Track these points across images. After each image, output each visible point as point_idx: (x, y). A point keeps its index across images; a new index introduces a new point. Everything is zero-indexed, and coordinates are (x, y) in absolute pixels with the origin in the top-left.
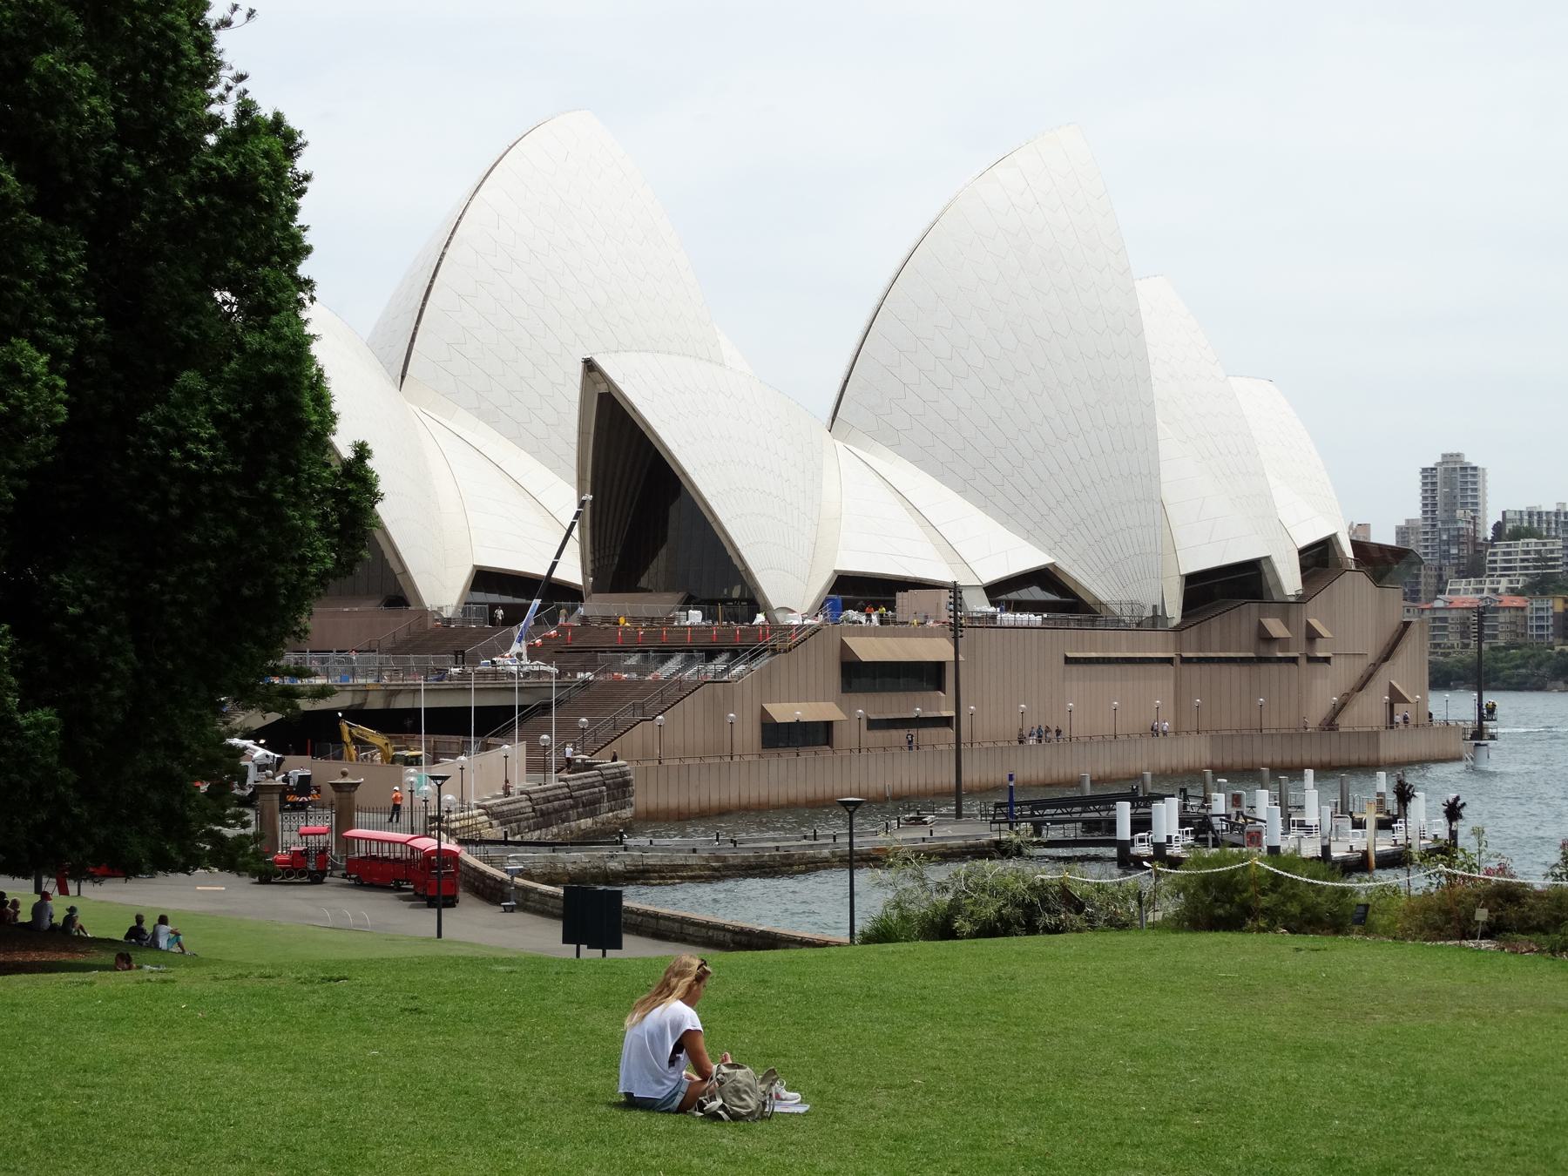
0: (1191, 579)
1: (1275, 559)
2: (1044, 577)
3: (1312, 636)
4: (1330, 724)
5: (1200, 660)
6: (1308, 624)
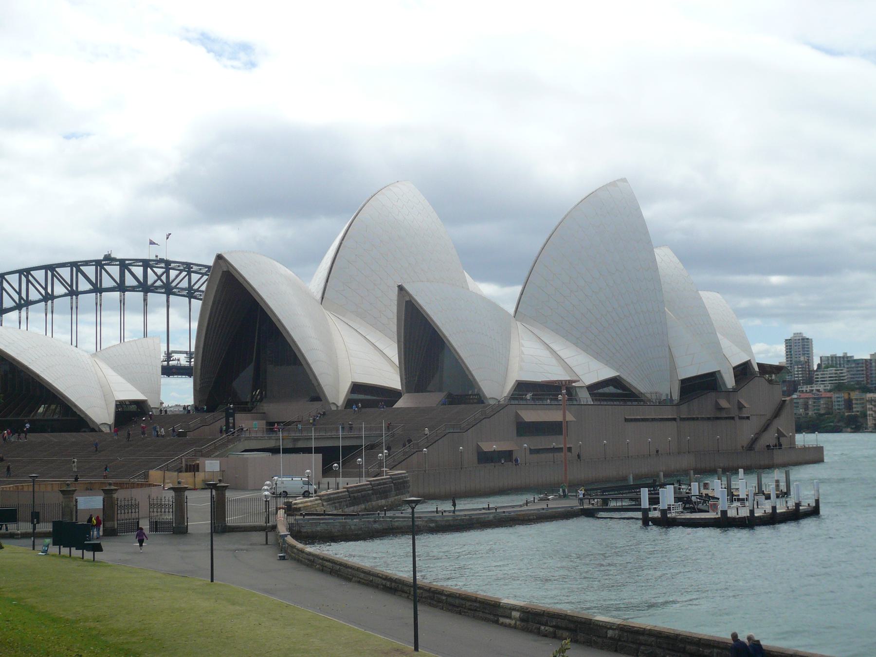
0: (683, 382)
1: (722, 372)
2: (615, 382)
3: (741, 407)
4: (751, 447)
5: (688, 419)
6: (739, 402)
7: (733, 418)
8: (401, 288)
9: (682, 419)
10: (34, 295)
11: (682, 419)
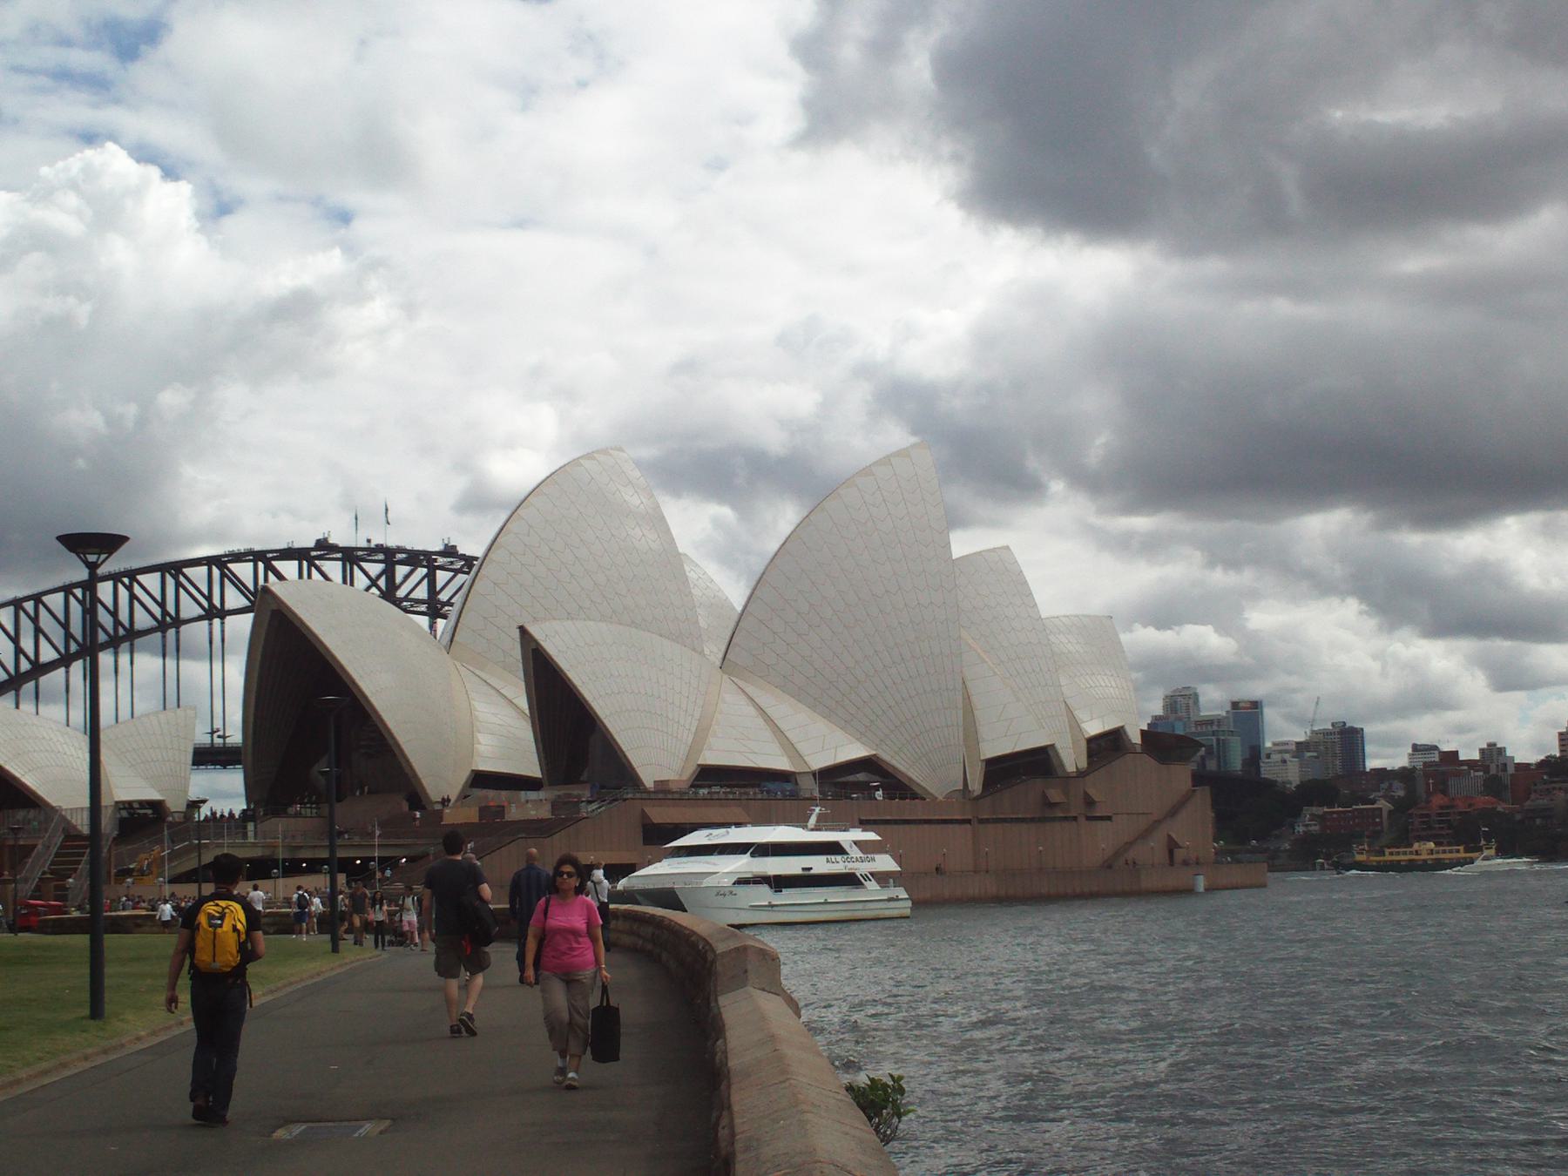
0: (990, 762)
1: (1058, 746)
3: (1089, 802)
4: (1108, 866)
6: (1086, 793)
7: (1075, 819)
8: (523, 631)
9: (982, 821)
10: (142, 620)
11: (982, 821)
